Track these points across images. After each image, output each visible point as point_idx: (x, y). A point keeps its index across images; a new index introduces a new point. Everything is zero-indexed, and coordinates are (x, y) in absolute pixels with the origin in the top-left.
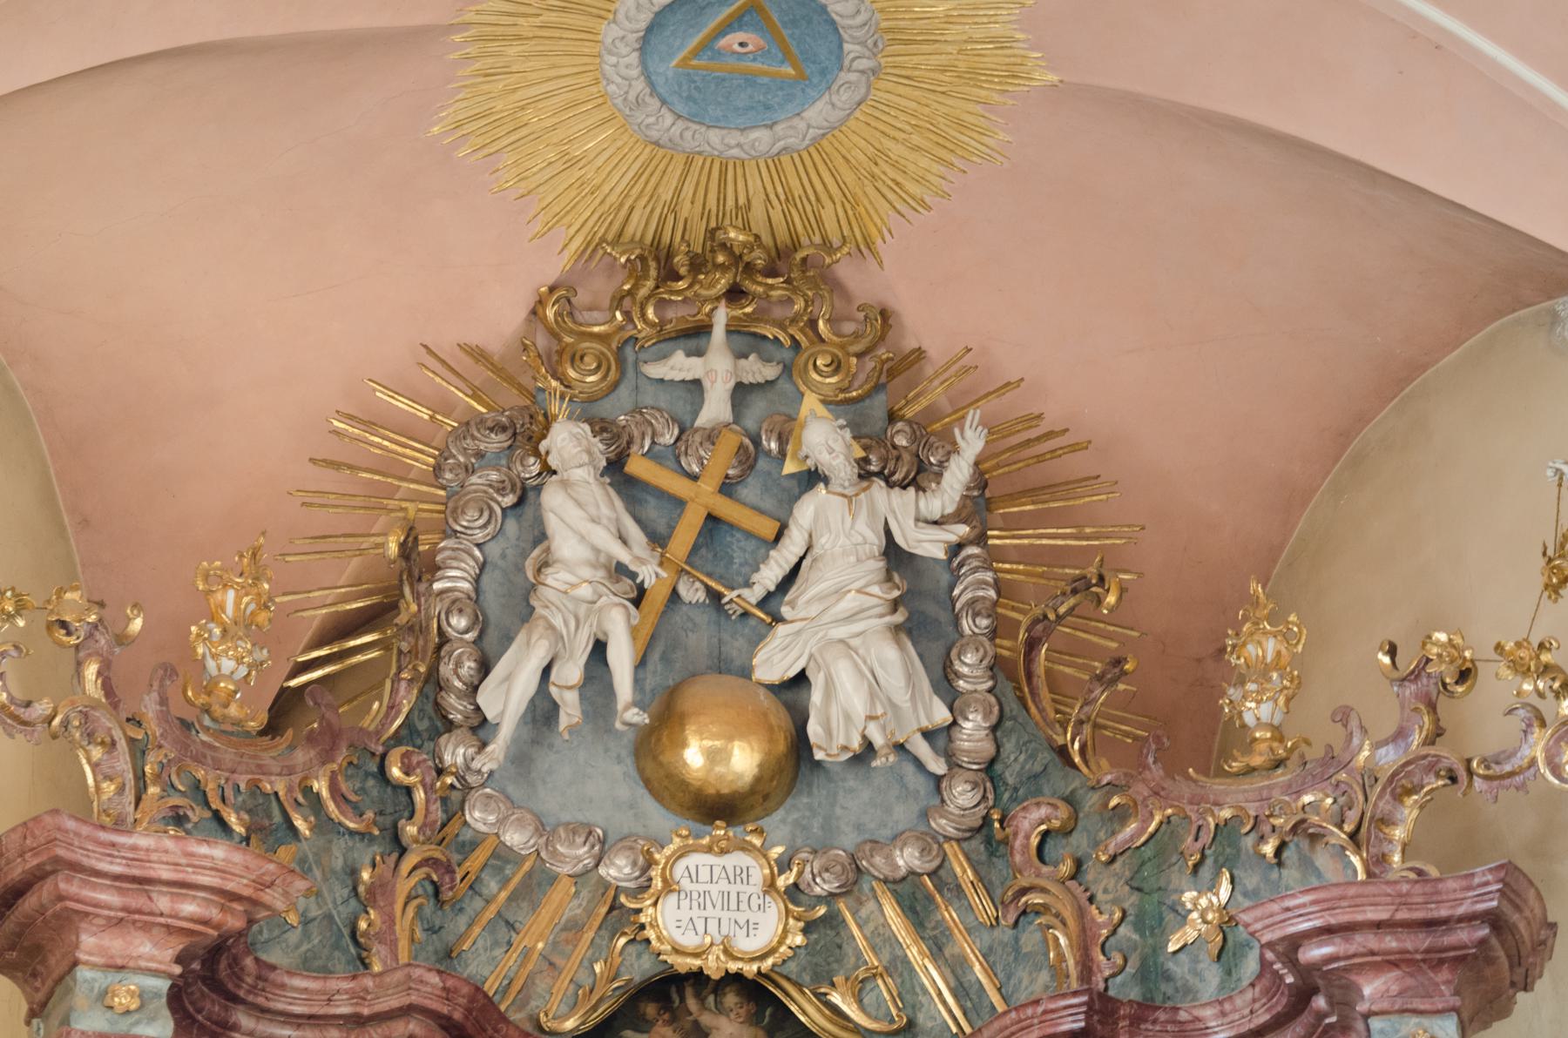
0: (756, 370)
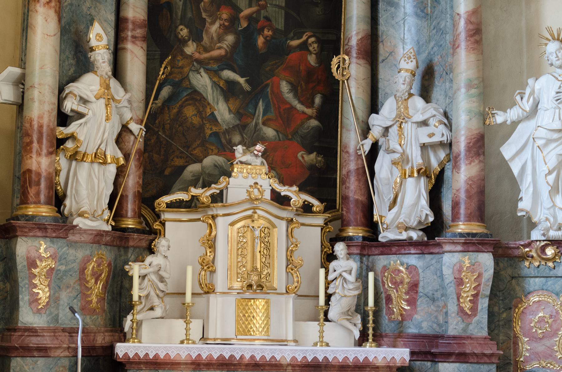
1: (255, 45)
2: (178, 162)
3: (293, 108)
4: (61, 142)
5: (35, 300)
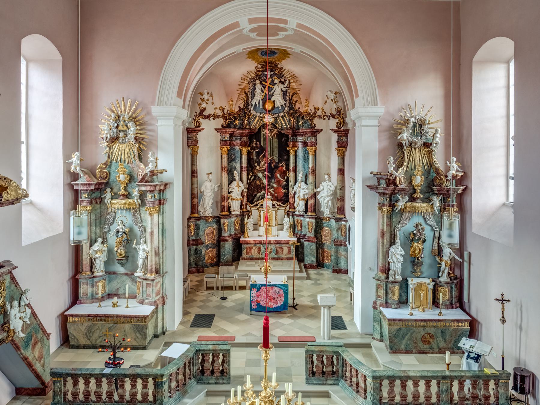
0: (272, 73)
1: (271, 166)
2: (256, 193)
3: (280, 180)
4: (229, 197)
5: (225, 231)
